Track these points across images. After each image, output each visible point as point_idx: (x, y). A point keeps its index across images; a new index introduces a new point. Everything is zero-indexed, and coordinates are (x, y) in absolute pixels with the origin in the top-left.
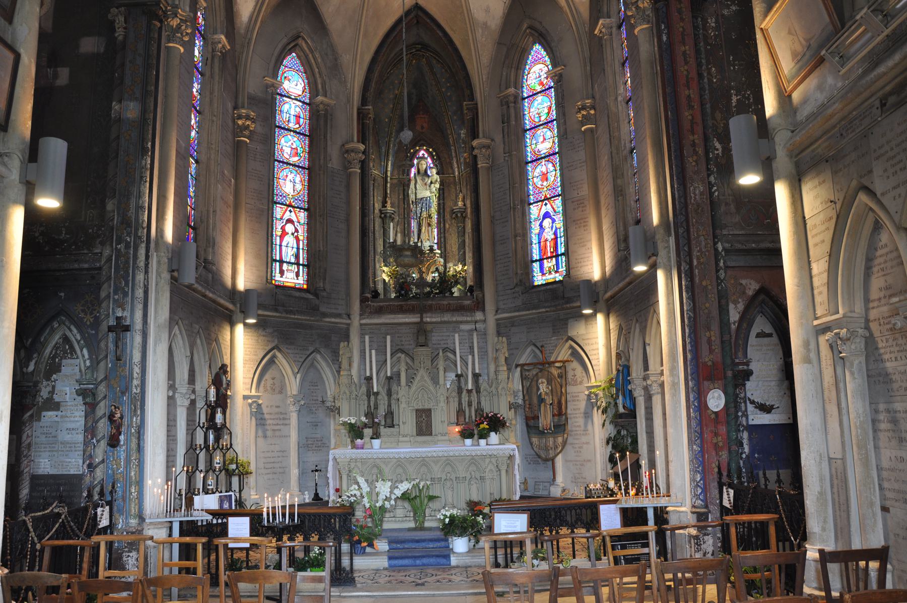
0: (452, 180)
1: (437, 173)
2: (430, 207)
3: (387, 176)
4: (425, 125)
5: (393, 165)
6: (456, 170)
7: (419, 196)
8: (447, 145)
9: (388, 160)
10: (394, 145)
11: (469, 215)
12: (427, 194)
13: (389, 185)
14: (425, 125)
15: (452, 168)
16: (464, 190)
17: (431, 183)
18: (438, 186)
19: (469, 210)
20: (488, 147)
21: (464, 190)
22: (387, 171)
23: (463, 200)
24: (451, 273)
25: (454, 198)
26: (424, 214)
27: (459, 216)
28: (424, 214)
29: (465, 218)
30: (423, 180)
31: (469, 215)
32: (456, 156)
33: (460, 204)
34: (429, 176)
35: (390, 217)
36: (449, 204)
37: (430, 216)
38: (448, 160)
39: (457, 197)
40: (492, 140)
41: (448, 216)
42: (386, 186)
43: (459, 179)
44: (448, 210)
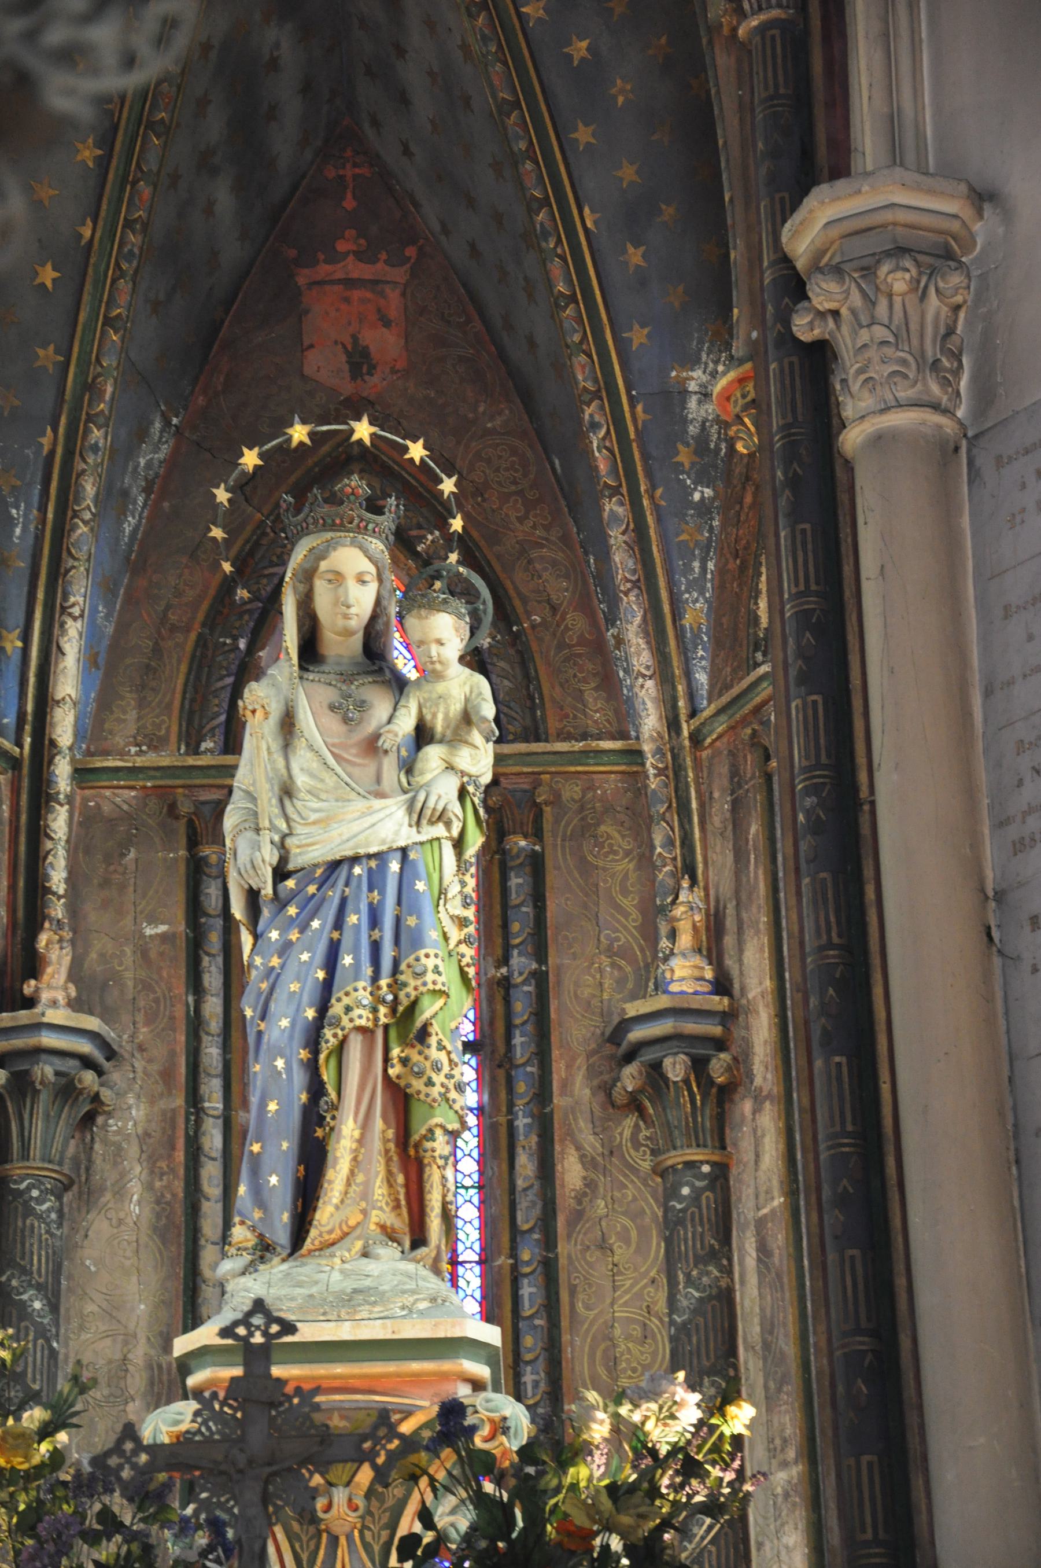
0: (610, 782)
1: (475, 659)
2: (406, 939)
3: (44, 749)
4: (385, 343)
5: (106, 664)
6: (647, 694)
7: (312, 849)
8: (572, 498)
9: (55, 613)
10: (114, 499)
11: (763, 1072)
12: (387, 825)
13: (59, 822)
14: (385, 343)
15: (609, 683)
16: (717, 861)
17: (423, 735)
18: (479, 760)
19: (761, 1031)
20: (937, 254)
21: (717, 861)
22: (45, 702)
23: (713, 942)
24: (590, 1473)
25: (625, 932)
26: (358, 1003)
27: (678, 1083)
28: (358, 1003)
29: (724, 1096)
30: (349, 711)
31: (763, 1072)
32: (647, 583)
33: (685, 973)
34: (399, 685)
35: (67, 1090)
36: (587, 987)
37: (406, 1024)
38: (576, 623)
39: (654, 913)
40: (982, 197)
41: (575, 1090)
42: (37, 832)
43: (675, 772)
44: (575, 1033)
